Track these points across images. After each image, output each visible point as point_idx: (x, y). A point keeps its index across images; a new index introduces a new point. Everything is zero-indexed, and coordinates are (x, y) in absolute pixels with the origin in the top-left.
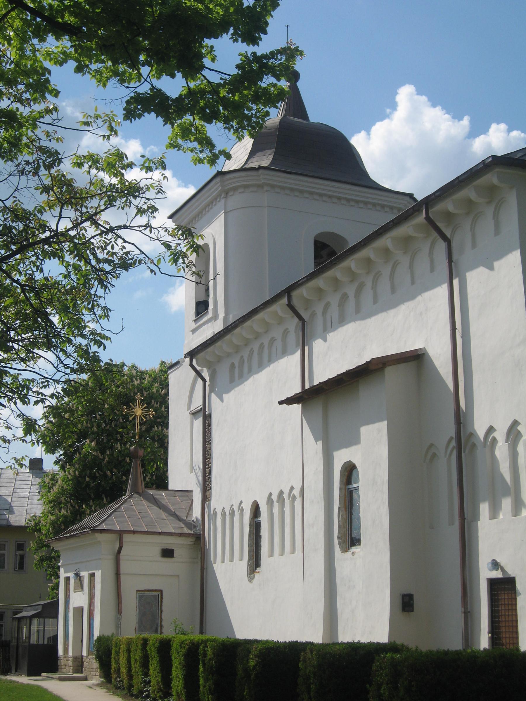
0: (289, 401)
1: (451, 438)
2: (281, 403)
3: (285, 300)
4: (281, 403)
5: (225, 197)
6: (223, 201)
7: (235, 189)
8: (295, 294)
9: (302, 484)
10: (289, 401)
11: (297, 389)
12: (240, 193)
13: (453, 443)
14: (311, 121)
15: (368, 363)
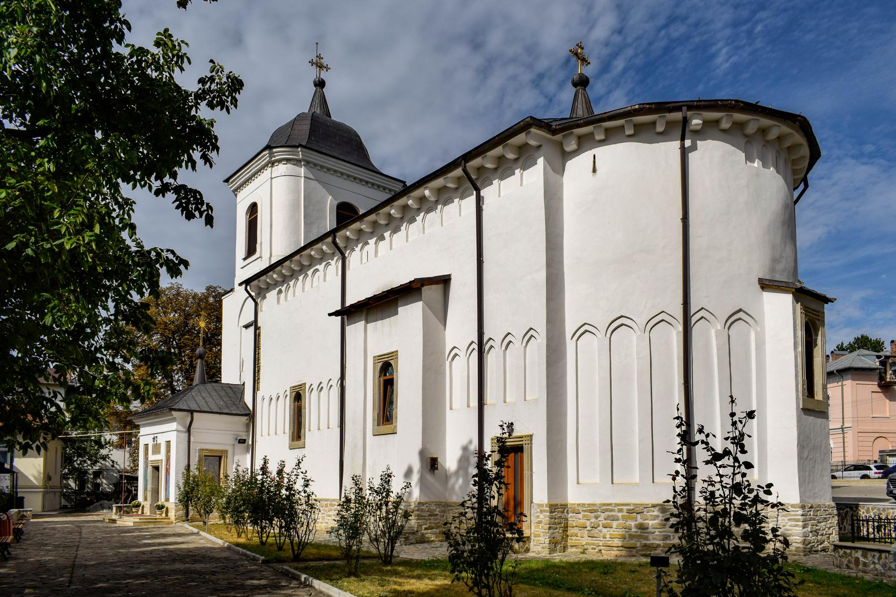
0: (336, 314)
1: (473, 342)
2: (330, 315)
3: (330, 239)
4: (330, 315)
5: (272, 166)
6: (269, 169)
7: (280, 161)
8: (339, 234)
9: (339, 376)
10: (336, 314)
11: (339, 308)
12: (284, 164)
13: (475, 346)
14: (333, 118)
15: (411, 282)
